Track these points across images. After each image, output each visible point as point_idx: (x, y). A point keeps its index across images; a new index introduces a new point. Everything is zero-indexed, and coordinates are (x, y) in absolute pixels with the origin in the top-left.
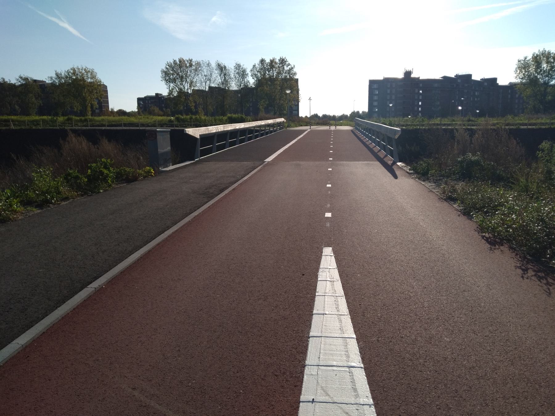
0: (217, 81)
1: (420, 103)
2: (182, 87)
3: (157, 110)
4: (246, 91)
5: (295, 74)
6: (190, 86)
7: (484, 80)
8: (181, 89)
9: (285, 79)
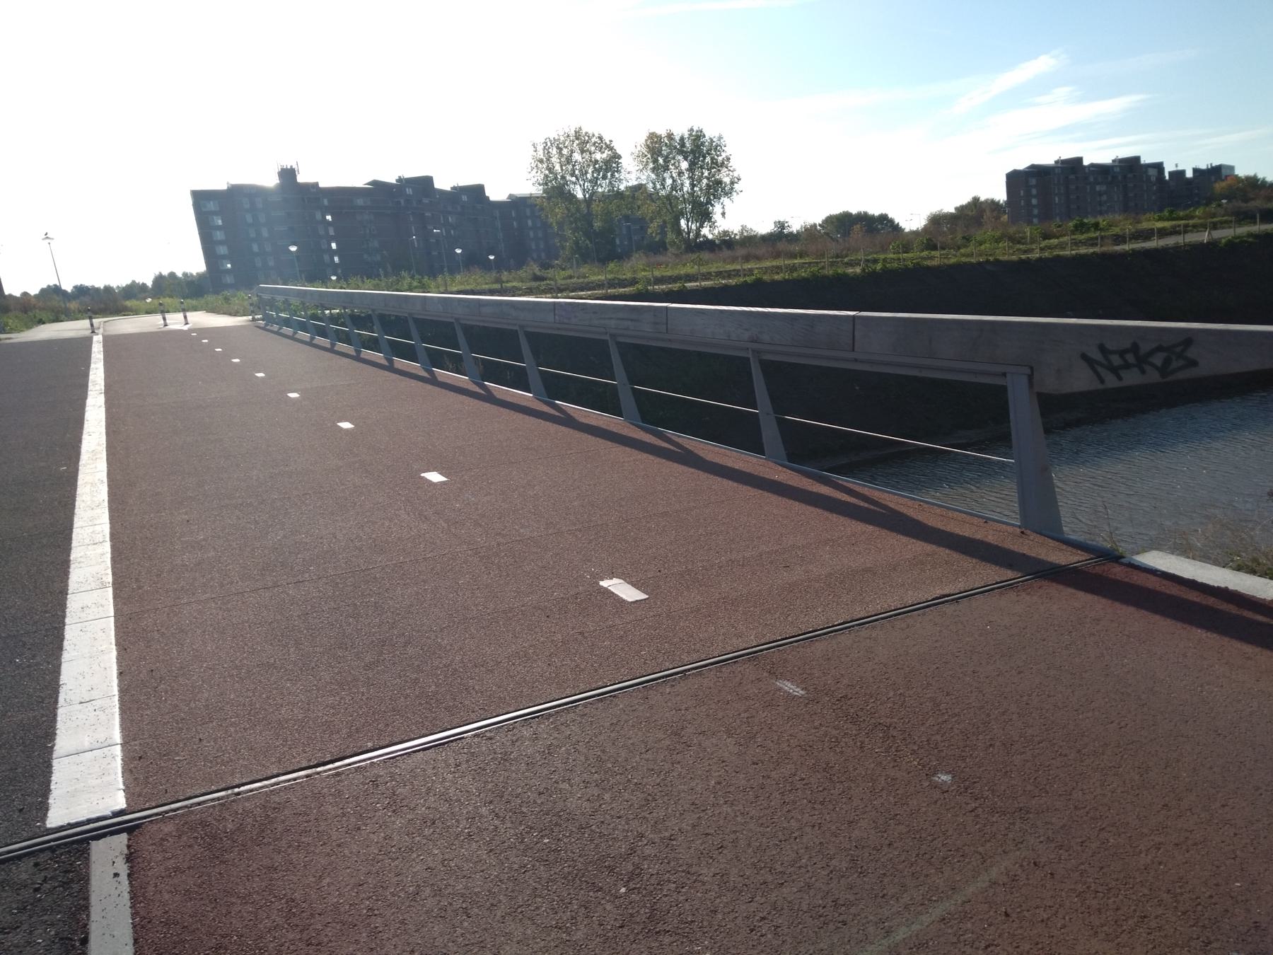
1: (334, 246)
7: (459, 191)
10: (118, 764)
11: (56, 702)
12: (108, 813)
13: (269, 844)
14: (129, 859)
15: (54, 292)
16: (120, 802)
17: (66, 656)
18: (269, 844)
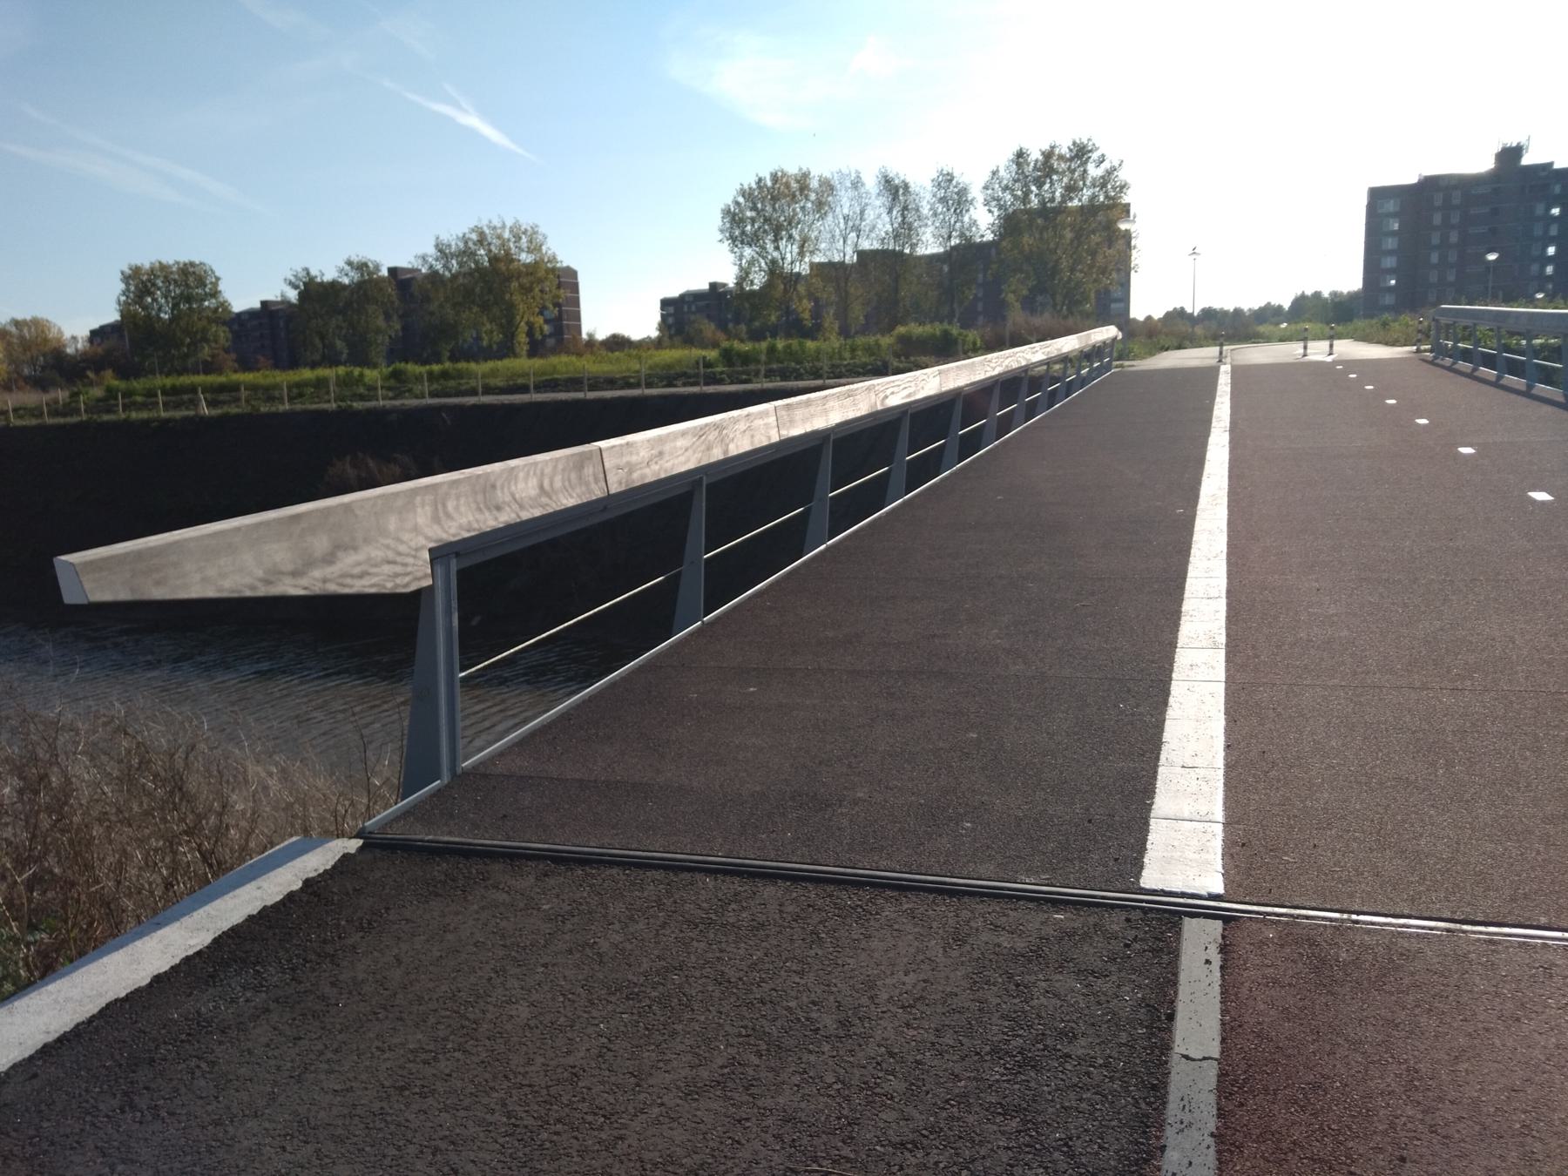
0: (878, 230)
2: (776, 254)
3: (709, 329)
4: (966, 257)
5: (1123, 187)
6: (801, 254)
8: (774, 262)
9: (1091, 209)
10: (1217, 844)
11: (1158, 758)
12: (1204, 893)
13: (1392, 994)
14: (1224, 949)
15: (1178, 315)
16: (1218, 887)
17: (1171, 713)
18: (1392, 994)
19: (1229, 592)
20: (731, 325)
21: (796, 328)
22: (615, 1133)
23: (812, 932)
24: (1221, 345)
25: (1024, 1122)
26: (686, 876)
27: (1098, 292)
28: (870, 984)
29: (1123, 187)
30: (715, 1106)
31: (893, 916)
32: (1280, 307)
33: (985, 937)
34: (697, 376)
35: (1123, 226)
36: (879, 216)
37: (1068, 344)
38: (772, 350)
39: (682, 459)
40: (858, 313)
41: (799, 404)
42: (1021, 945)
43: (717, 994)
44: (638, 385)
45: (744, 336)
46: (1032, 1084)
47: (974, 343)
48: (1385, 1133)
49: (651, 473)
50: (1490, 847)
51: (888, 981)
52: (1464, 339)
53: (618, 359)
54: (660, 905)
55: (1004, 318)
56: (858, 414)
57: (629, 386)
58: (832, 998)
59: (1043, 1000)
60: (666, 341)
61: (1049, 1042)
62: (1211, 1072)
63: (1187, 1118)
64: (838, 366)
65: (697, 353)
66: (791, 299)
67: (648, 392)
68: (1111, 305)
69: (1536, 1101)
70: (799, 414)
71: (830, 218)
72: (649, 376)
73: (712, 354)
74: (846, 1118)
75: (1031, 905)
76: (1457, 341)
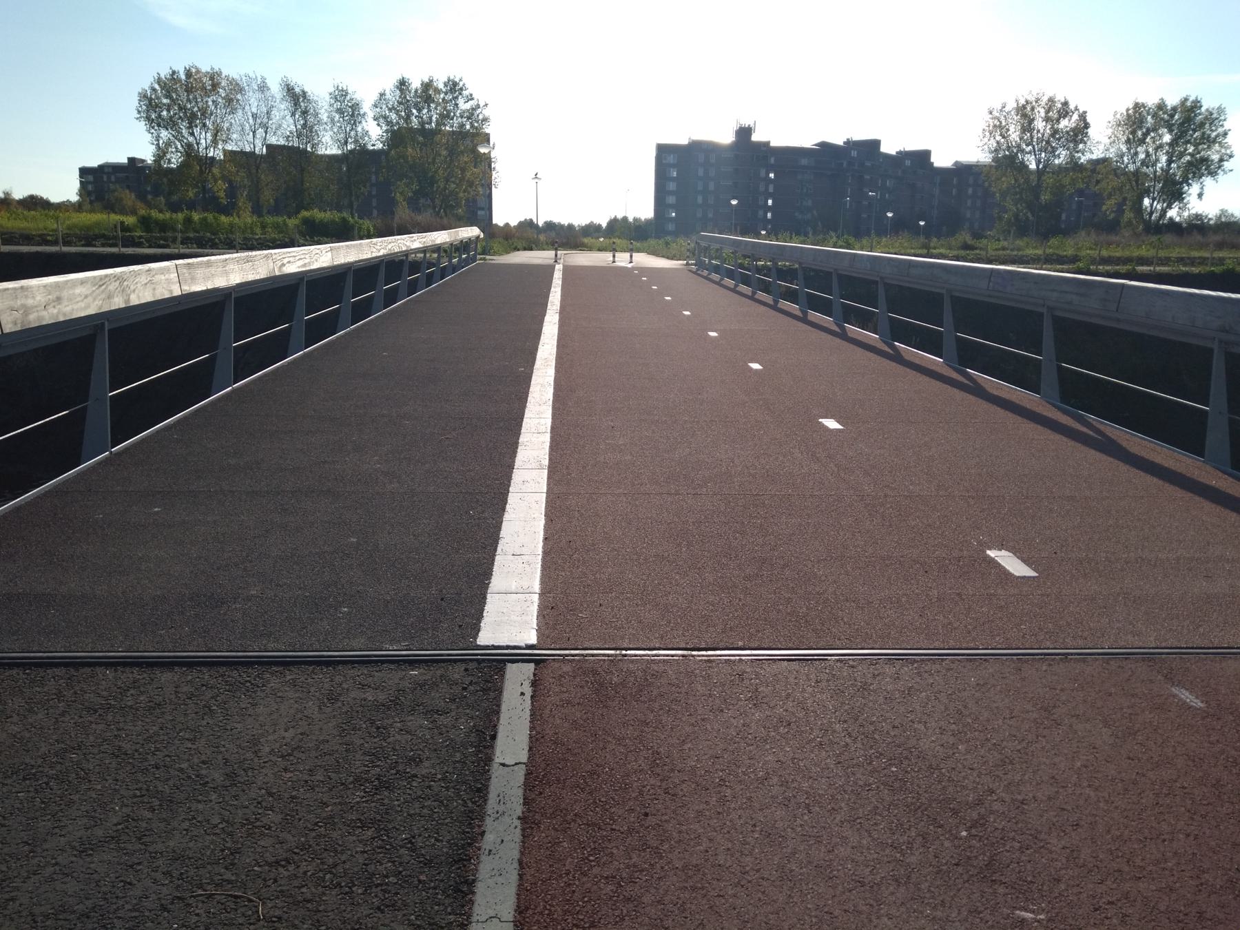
0: (283, 129)
1: (770, 202)
2: (191, 139)
3: (129, 198)
4: (359, 160)
5: (485, 120)
6: (215, 142)
7: (904, 155)
8: (189, 145)
9: (461, 134)
10: (535, 608)
11: (495, 550)
12: (523, 644)
13: (645, 702)
14: (534, 684)
15: (528, 225)
16: (533, 639)
17: (507, 516)
18: (645, 702)
19: (552, 428)
20: (150, 197)
21: (210, 203)
22: (7, 896)
23: (205, 706)
24: (556, 250)
25: (378, 830)
26: (88, 670)
27: (467, 200)
28: (255, 742)
29: (485, 120)
30: (106, 857)
31: (277, 686)
32: (600, 226)
33: (353, 694)
34: (115, 238)
35: (483, 150)
36: (284, 117)
37: (441, 237)
38: (188, 221)
39: (83, 305)
40: (268, 196)
41: (200, 264)
42: (382, 697)
43: (114, 765)
44: (55, 243)
45: (163, 206)
46: (386, 801)
47: (369, 231)
48: (636, 799)
49: (49, 316)
50: (711, 598)
51: (271, 738)
52: (716, 258)
53: (34, 218)
54: (59, 695)
55: (393, 213)
56: (258, 277)
57: (47, 243)
58: (220, 757)
59: (398, 737)
60: (87, 206)
61: (400, 768)
62: (521, 772)
63: (501, 808)
64: (249, 239)
65: (115, 218)
66: (206, 181)
67: (66, 249)
68: (479, 210)
69: (729, 762)
70: (199, 273)
71: (240, 112)
72: (68, 235)
73: (130, 220)
74: (229, 849)
75: (392, 667)
76: (711, 258)
